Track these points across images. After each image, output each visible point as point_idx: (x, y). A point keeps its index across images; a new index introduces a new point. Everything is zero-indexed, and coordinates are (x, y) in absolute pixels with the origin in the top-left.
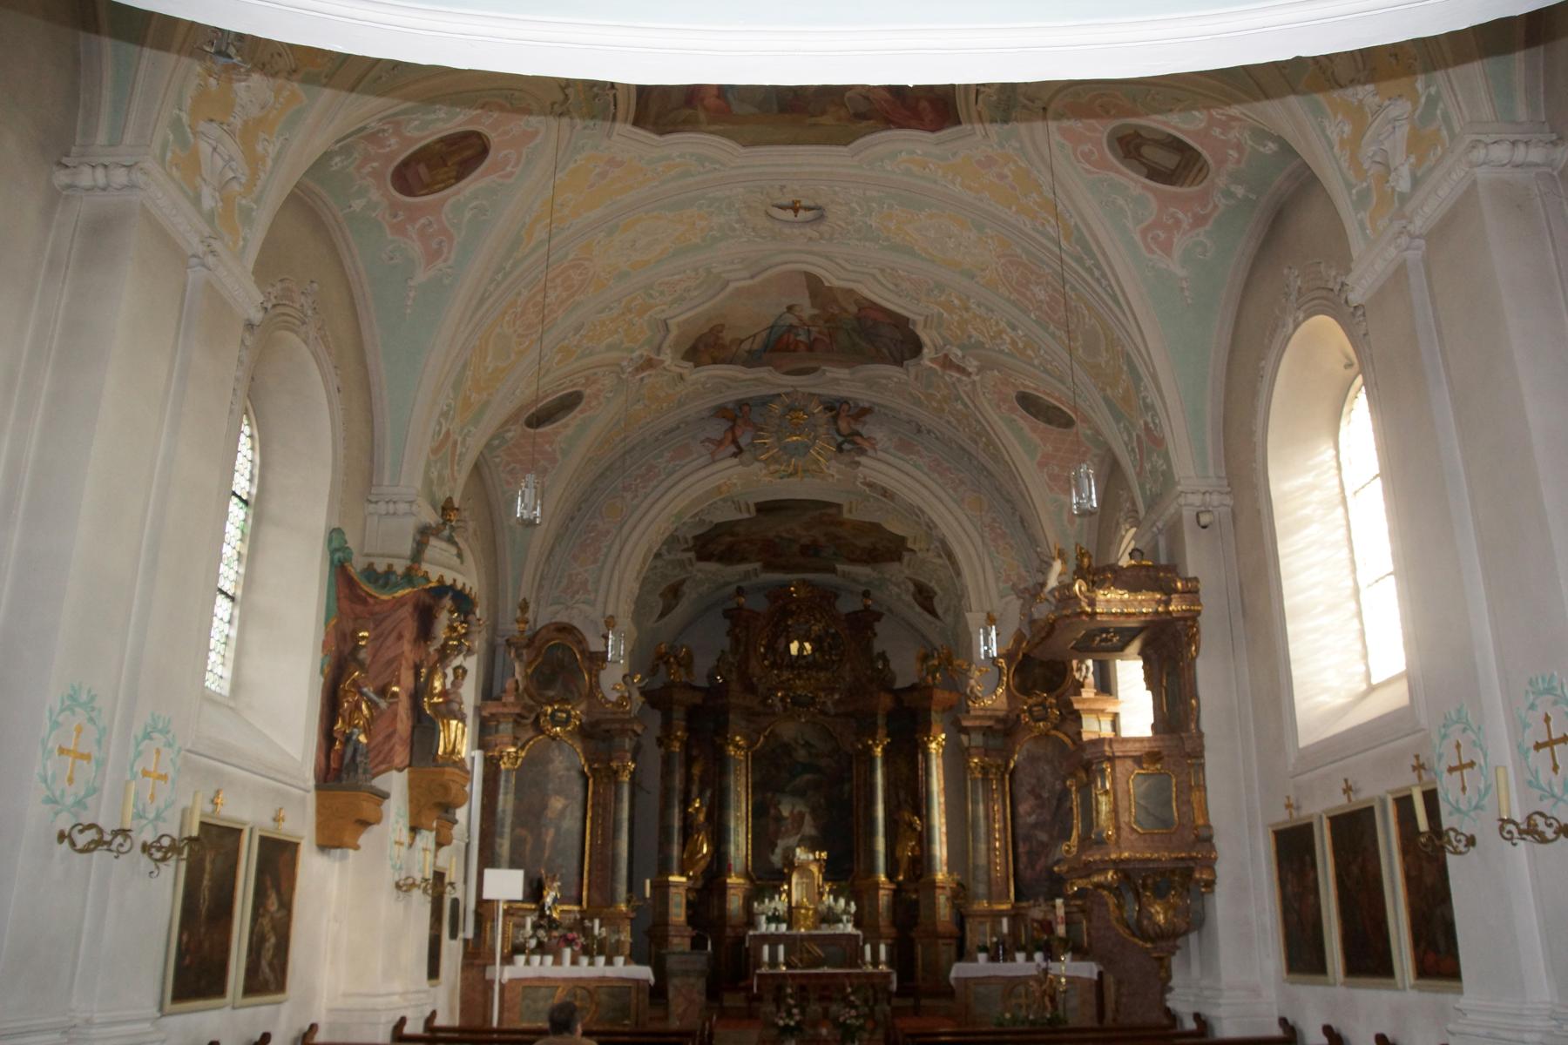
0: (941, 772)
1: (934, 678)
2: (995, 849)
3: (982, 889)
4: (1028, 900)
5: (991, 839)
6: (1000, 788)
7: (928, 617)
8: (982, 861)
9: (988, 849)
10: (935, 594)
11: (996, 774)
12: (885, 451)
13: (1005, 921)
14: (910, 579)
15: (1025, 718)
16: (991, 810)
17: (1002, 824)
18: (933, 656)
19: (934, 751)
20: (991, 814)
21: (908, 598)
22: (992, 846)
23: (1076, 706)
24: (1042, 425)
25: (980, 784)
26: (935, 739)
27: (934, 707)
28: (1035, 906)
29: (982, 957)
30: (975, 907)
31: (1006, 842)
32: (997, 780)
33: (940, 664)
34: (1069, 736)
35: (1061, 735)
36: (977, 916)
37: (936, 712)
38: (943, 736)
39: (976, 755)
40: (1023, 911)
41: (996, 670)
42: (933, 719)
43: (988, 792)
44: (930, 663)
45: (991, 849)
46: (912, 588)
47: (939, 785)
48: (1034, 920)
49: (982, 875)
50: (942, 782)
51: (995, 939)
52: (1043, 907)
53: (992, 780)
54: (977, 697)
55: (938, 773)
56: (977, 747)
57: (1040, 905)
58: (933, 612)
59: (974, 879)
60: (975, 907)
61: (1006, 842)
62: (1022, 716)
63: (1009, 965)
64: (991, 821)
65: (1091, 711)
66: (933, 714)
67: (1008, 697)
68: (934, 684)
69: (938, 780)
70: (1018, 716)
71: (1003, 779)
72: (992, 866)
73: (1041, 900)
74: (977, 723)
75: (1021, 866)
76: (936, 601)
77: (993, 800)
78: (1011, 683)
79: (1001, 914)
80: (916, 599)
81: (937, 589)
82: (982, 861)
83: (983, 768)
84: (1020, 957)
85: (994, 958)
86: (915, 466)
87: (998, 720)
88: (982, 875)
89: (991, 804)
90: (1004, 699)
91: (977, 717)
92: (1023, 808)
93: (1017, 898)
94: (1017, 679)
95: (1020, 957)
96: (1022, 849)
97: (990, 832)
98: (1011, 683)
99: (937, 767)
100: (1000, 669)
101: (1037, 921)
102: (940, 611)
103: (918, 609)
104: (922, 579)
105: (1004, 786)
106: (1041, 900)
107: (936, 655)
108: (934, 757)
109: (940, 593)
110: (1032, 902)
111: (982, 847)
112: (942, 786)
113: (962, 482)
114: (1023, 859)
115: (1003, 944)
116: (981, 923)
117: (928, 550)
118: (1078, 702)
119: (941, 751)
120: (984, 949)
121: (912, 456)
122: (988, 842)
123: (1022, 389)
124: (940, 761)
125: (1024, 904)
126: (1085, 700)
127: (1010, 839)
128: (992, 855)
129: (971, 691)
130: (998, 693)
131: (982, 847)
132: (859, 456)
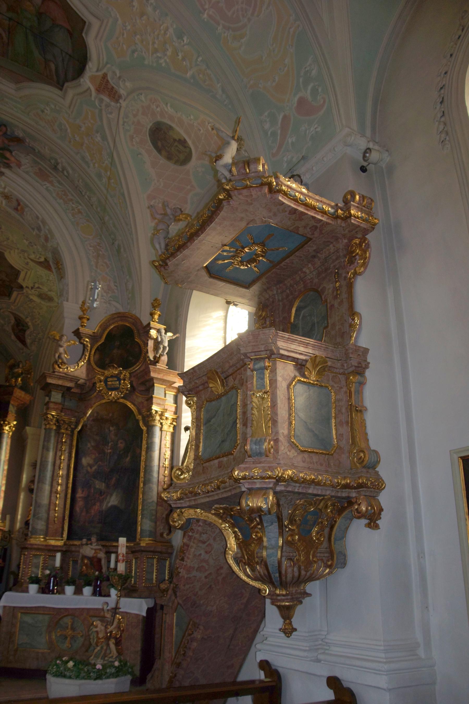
0: (9, 448)
1: (17, 380)
2: (57, 492)
3: (41, 525)
4: (81, 539)
5: (55, 483)
6: (68, 442)
7: (20, 345)
8: (45, 501)
9: (51, 492)
10: (28, 328)
11: (67, 429)
12: (27, 173)
13: (58, 555)
14: (13, 314)
15: (100, 386)
16: (57, 458)
17: (65, 473)
18: (19, 366)
19: (6, 432)
20: (58, 462)
21: (8, 329)
22: (54, 490)
23: (153, 374)
24: (162, 161)
25: (53, 434)
26: (9, 424)
27: (12, 402)
28: (87, 544)
29: (33, 588)
30: (32, 541)
31: (67, 487)
32: (67, 434)
33: (22, 373)
34: (134, 405)
35: (129, 404)
36: (31, 549)
37: (13, 405)
38: (15, 423)
39: (55, 409)
40: (73, 549)
41: (82, 345)
42: (10, 409)
43: (59, 442)
44: (16, 370)
45: (52, 491)
46: (13, 321)
47: (6, 457)
48: (84, 557)
49: (43, 514)
50: (8, 455)
51: (48, 572)
52: (94, 546)
53: (63, 434)
54: (63, 363)
55: (6, 448)
56: (55, 403)
57: (91, 544)
58: (23, 342)
59: (34, 516)
60: (32, 541)
61: (67, 487)
62: (98, 385)
63: (57, 597)
64: (57, 468)
65: (163, 381)
66: (11, 406)
67: (88, 369)
68: (16, 385)
69: (6, 453)
70: (94, 384)
71: (72, 436)
72: (52, 507)
73: (94, 539)
74: (60, 382)
75: (77, 509)
76: (28, 332)
77: (61, 450)
78: (92, 358)
79: (53, 550)
80: (13, 330)
81: (30, 324)
82: (45, 501)
83: (57, 421)
84: (69, 590)
85: (44, 590)
86: (47, 189)
87: (78, 386)
88: (43, 514)
89: (59, 453)
90: (84, 370)
91: (60, 378)
92: (85, 461)
93: (69, 538)
94: (97, 356)
95: (69, 590)
96: (80, 494)
97: (54, 476)
98: (92, 358)
99: (7, 444)
100: (85, 347)
101: (89, 558)
102: (28, 341)
103: (13, 337)
104: (22, 316)
105: (72, 441)
106: (94, 539)
107: (21, 366)
108: (5, 436)
109: (32, 328)
110: (84, 541)
111: (47, 488)
112: (7, 458)
113: (80, 212)
114: (80, 504)
115: (55, 577)
116: (35, 556)
117: (32, 288)
118: (155, 371)
119: (11, 434)
120: (35, 581)
121: (46, 183)
122: (52, 486)
123: (159, 119)
124: (9, 441)
125: (77, 543)
126: (160, 371)
127: (70, 485)
128: (53, 498)
129: (59, 357)
130: (80, 365)
131: (47, 488)
132: (4, 168)
